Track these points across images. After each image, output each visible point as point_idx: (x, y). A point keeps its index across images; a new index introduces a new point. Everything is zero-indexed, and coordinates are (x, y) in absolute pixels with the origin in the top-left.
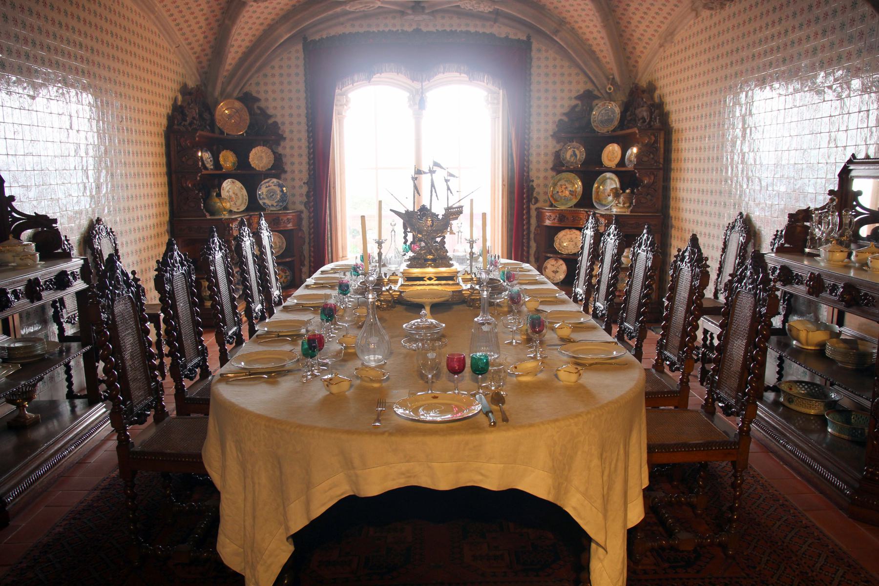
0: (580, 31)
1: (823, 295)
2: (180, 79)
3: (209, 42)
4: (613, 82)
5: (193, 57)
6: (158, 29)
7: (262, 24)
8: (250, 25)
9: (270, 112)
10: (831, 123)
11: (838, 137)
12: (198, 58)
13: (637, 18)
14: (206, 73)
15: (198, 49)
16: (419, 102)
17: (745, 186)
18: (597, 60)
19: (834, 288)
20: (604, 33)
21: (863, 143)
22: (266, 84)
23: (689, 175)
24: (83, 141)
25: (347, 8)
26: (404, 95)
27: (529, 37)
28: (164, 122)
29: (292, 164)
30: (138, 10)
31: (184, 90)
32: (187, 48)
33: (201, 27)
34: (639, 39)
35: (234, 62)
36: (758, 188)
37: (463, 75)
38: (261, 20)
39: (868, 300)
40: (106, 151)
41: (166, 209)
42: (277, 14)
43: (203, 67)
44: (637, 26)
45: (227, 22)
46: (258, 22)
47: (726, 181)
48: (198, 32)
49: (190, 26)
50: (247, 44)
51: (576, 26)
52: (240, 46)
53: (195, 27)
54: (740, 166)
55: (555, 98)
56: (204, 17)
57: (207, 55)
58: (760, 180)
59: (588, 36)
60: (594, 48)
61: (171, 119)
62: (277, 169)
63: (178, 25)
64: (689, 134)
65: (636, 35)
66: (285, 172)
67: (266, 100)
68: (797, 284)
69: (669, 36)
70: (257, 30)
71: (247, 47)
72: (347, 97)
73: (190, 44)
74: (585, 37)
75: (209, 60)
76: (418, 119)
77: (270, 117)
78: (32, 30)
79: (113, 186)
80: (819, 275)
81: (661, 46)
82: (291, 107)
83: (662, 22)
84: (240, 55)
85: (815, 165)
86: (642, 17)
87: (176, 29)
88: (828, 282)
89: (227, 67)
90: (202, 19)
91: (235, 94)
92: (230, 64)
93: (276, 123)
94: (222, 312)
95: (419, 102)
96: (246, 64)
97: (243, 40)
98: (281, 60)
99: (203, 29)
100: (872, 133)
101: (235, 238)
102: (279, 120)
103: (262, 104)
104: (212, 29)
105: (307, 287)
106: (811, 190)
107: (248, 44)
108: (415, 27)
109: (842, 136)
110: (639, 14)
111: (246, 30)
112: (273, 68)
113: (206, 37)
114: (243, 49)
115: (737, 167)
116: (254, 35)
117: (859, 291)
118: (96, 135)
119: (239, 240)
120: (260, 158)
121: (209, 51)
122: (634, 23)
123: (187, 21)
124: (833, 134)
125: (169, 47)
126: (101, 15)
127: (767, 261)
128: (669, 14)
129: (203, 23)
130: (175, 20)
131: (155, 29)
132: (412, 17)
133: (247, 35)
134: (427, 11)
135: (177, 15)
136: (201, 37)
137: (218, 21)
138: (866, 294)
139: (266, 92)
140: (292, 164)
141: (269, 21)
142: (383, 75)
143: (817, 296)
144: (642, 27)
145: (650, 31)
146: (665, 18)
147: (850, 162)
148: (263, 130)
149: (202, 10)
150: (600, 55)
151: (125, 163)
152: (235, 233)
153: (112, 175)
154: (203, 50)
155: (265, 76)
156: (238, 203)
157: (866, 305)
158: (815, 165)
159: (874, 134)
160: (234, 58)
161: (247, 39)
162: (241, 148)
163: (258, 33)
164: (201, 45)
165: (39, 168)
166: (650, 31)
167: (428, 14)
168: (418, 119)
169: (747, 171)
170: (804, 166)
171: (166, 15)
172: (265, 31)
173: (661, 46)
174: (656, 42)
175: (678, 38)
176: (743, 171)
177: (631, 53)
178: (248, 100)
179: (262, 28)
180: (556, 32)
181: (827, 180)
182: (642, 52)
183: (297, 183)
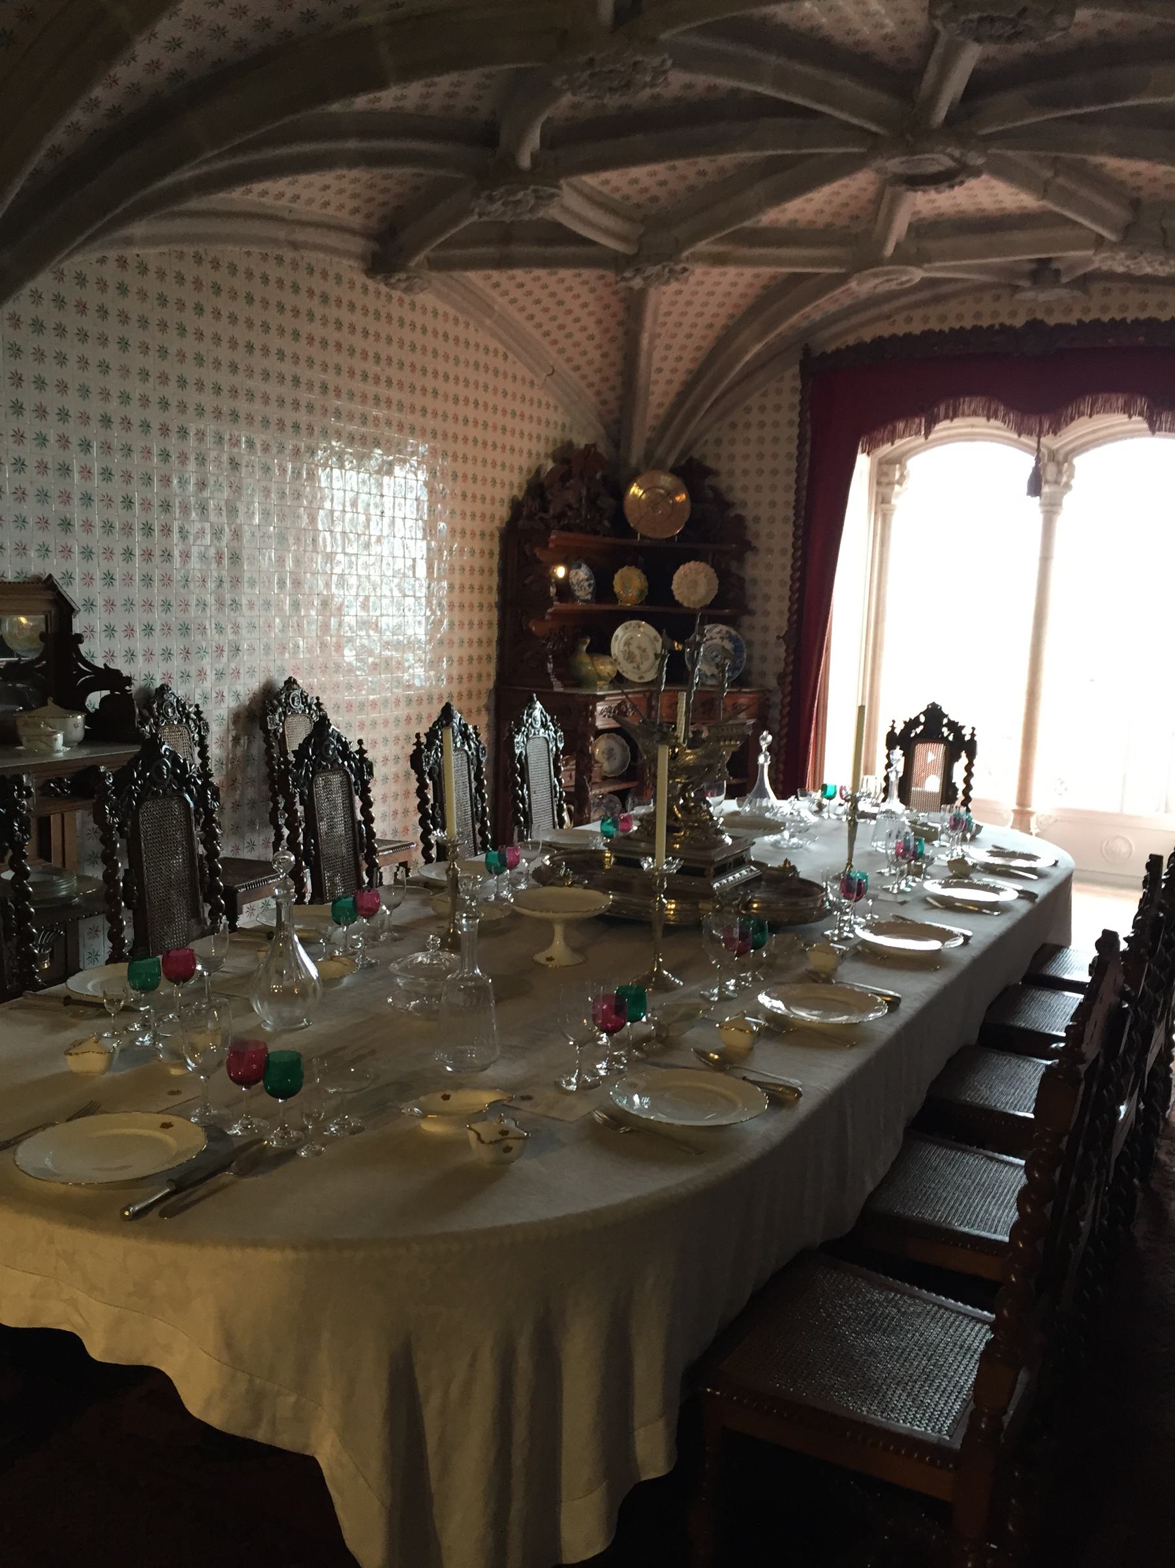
2: (555, 434)
3: (613, 364)
5: (590, 393)
6: (502, 341)
7: (711, 326)
9: (737, 496)
12: (598, 393)
15: (595, 378)
22: (732, 442)
28: (503, 512)
29: (767, 598)
30: (452, 312)
31: (565, 455)
32: (576, 376)
35: (668, 400)
37: (1136, 418)
38: (707, 320)
41: (491, 669)
42: (736, 306)
50: (686, 365)
53: (579, 337)
56: (593, 319)
61: (516, 506)
62: (730, 604)
66: (751, 613)
67: (731, 473)
70: (704, 338)
71: (690, 372)
73: (577, 368)
76: (1051, 510)
77: (729, 505)
84: (676, 387)
90: (590, 322)
91: (671, 462)
92: (660, 405)
93: (740, 519)
97: (679, 359)
98: (765, 395)
99: (597, 341)
102: (748, 513)
103: (723, 483)
104: (613, 340)
107: (690, 366)
112: (748, 410)
113: (605, 355)
114: (680, 377)
116: (699, 348)
120: (692, 583)
125: (529, 376)
129: (593, 329)
130: (539, 326)
131: (493, 344)
132: (1030, 295)
134: (1064, 280)
136: (595, 355)
139: (732, 457)
140: (767, 598)
141: (720, 322)
142: (957, 422)
148: (715, 529)
149: (585, 305)
154: (605, 380)
156: (644, 667)
160: (666, 393)
162: (659, 563)
163: (704, 344)
164: (600, 370)
167: (1067, 285)
178: (692, 473)
179: (712, 334)
183: (772, 637)
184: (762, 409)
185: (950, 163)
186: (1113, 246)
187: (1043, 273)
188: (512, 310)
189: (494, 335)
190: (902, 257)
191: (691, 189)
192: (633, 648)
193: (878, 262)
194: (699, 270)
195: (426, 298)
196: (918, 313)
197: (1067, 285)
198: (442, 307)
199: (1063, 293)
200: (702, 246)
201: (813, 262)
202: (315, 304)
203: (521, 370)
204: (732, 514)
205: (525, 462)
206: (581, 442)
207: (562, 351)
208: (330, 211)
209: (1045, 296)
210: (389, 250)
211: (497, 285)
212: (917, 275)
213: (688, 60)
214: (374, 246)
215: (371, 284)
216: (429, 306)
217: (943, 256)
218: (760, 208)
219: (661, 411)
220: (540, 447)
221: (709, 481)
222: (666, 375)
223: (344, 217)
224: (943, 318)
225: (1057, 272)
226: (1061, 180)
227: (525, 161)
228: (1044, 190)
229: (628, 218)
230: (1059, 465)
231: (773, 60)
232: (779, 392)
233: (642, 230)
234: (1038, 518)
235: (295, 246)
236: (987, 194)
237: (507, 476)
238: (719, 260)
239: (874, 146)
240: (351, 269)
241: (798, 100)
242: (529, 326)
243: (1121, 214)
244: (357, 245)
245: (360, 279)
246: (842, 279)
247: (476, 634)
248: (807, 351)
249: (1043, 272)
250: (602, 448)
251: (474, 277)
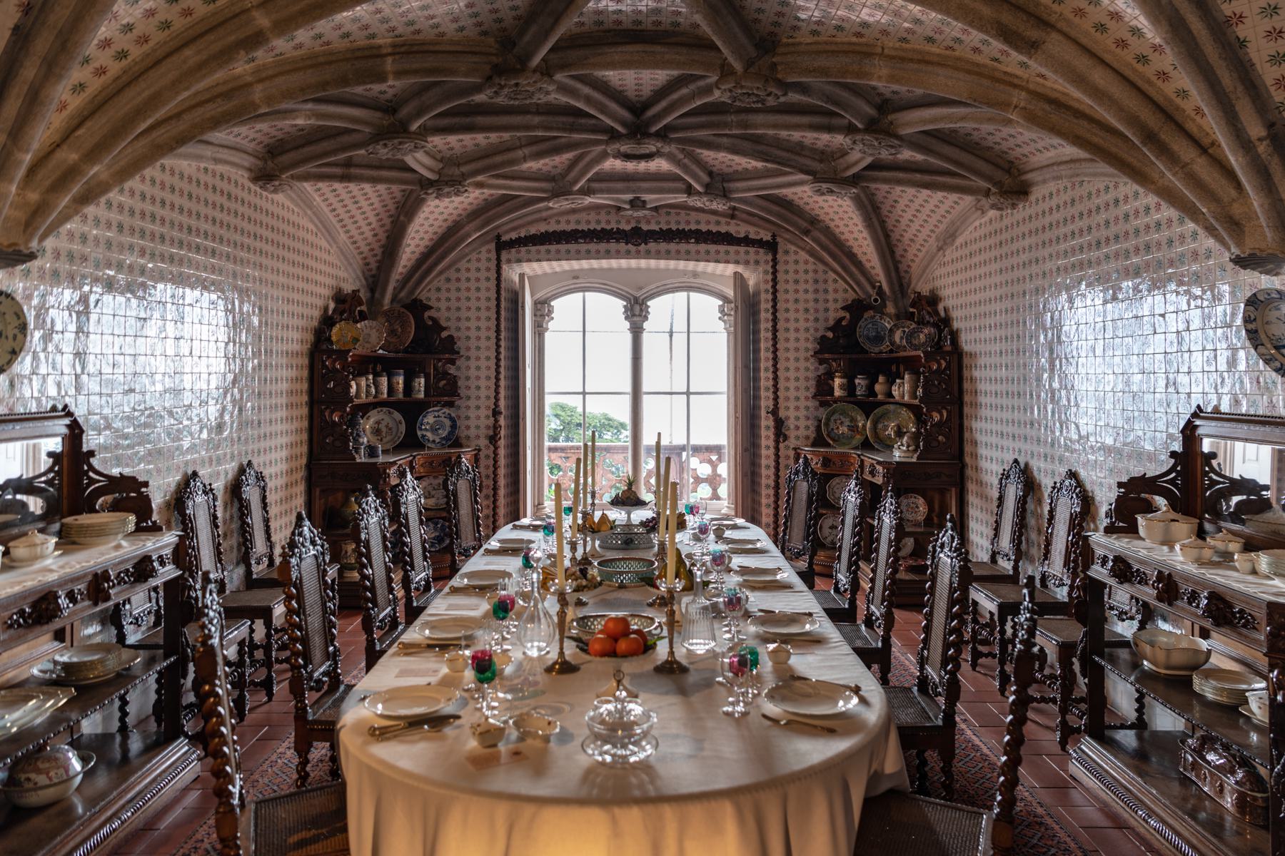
0: (837, 231)
1: (1179, 603)
4: (880, 291)
6: (316, 226)
7: (446, 220)
8: (431, 221)
10: (1168, 362)
11: (1179, 380)
13: (908, 216)
14: (373, 276)
15: (365, 249)
16: (636, 312)
17: (1058, 434)
18: (859, 265)
19: (1194, 597)
20: (865, 234)
21: (1213, 391)
23: (984, 412)
24: (204, 370)
25: (551, 205)
26: (617, 306)
27: (774, 236)
30: (292, 206)
32: (352, 247)
33: (370, 224)
34: (912, 240)
35: (409, 264)
36: (1075, 437)
38: (445, 216)
39: (1248, 621)
40: (234, 381)
43: (370, 270)
44: (908, 226)
45: (402, 218)
46: (441, 218)
47: (1032, 424)
48: (365, 229)
49: (356, 222)
51: (832, 225)
52: (418, 246)
53: (362, 223)
54: (1050, 407)
55: (807, 310)
57: (375, 255)
58: (1077, 427)
59: (847, 236)
60: (855, 250)
63: (341, 221)
64: (982, 361)
65: (908, 236)
68: (1140, 583)
69: (949, 238)
71: (427, 247)
72: (549, 305)
73: (355, 243)
74: (843, 237)
75: (379, 261)
76: (637, 332)
78: (153, 240)
79: (240, 424)
80: (1170, 575)
81: (940, 249)
82: (478, 319)
83: (939, 221)
84: (417, 255)
85: (1151, 414)
86: (914, 216)
87: (338, 226)
88: (1185, 588)
89: (400, 270)
94: (373, 589)
95: (636, 312)
96: (425, 267)
98: (469, 261)
100: (1223, 379)
101: (393, 488)
104: (382, 226)
105: (488, 552)
106: (1148, 447)
108: (633, 225)
109: (1183, 379)
110: (910, 213)
111: (426, 227)
112: (458, 270)
113: (375, 235)
114: (421, 249)
115: (1045, 408)
117: (1231, 606)
118: (223, 360)
119: (397, 491)
121: (379, 251)
122: (904, 222)
123: (352, 217)
124: (1171, 376)
126: (243, 215)
127: (1095, 547)
128: (948, 212)
129: (373, 219)
131: (311, 226)
133: (426, 232)
135: (340, 211)
136: (369, 234)
137: (391, 216)
138: (1241, 611)
141: (451, 219)
143: (1170, 604)
144: (915, 226)
145: (926, 231)
146: (943, 216)
147: (1198, 413)
150: (863, 259)
151: (259, 394)
152: (394, 481)
153: (240, 410)
155: (448, 280)
157: (1244, 626)
158: (1151, 414)
159: (1227, 380)
160: (409, 260)
161: (427, 237)
163: (440, 231)
164: (369, 244)
165: (142, 407)
166: (926, 231)
168: (637, 332)
169: (1060, 413)
170: (1136, 414)
171: (326, 210)
172: (449, 229)
173: (940, 249)
174: (933, 243)
175: (959, 241)
176: (1053, 412)
177: (902, 256)
179: (445, 225)
180: (807, 232)
181: (1170, 436)
182: (916, 255)
184: (468, 270)
185: (653, 149)
186: (699, 193)
187: (636, 204)
188: (323, 205)
189: (312, 221)
190: (587, 191)
191: (477, 145)
192: (382, 427)
193: (570, 193)
194: (470, 189)
195: (280, 197)
196: (563, 219)
197: (651, 209)
198: (288, 203)
199: (646, 212)
200: (479, 178)
201: (520, 189)
202: (224, 200)
203: (324, 243)
204: (444, 334)
205: (320, 303)
206: (348, 288)
207: (348, 232)
208: (238, 139)
209: (640, 213)
210: (272, 166)
211: (319, 190)
212: (589, 200)
213: (563, 89)
214: (259, 163)
215: (251, 185)
216: (280, 201)
217: (601, 191)
218: (525, 159)
219: (404, 271)
220: (327, 292)
221: (427, 314)
222: (412, 248)
223: (245, 144)
224: (578, 222)
225: (644, 202)
226: (686, 161)
227: (414, 127)
228: (678, 163)
229: (433, 157)
230: (641, 305)
231: (586, 90)
232: (479, 260)
233: (441, 166)
234: (628, 337)
235: (217, 161)
236: (661, 165)
237: (307, 311)
238: (480, 185)
239: (614, 136)
240: (242, 176)
241: (592, 112)
242: (330, 215)
243: (706, 179)
244: (247, 161)
245: (248, 184)
246: (547, 199)
247: (296, 425)
248: (499, 237)
249: (636, 204)
250: (362, 294)
251: (307, 186)
